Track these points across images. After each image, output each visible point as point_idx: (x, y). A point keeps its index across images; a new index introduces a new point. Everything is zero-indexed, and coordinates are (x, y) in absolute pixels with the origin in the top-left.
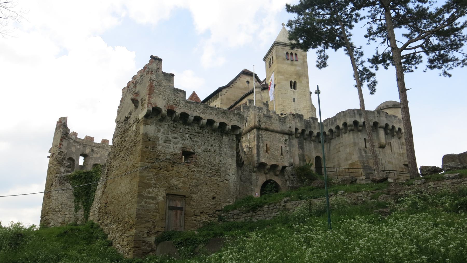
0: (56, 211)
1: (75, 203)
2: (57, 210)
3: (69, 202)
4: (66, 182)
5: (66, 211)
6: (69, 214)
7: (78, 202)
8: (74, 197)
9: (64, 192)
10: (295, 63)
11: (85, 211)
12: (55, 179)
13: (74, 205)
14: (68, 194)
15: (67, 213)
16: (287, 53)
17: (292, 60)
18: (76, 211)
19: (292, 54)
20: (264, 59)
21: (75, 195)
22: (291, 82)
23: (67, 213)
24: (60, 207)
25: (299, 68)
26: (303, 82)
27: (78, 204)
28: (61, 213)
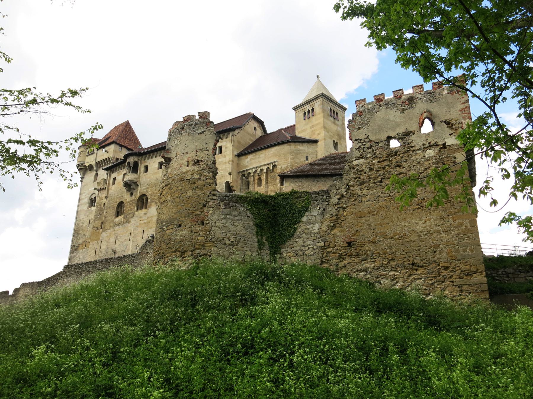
0: (225, 244)
1: (257, 237)
2: (227, 243)
3: (248, 234)
4: (237, 205)
5: (244, 246)
6: (250, 250)
7: (262, 236)
8: (255, 229)
9: (236, 218)
10: (337, 122)
11: (271, 250)
12: (210, 197)
13: (256, 240)
14: (245, 222)
15: (248, 249)
16: (331, 109)
17: (334, 119)
18: (260, 248)
19: (334, 112)
20: (295, 109)
21: (257, 225)
22: (334, 141)
23: (248, 249)
24: (232, 239)
25: (340, 129)
26: (343, 145)
27: (262, 239)
28: (236, 248)
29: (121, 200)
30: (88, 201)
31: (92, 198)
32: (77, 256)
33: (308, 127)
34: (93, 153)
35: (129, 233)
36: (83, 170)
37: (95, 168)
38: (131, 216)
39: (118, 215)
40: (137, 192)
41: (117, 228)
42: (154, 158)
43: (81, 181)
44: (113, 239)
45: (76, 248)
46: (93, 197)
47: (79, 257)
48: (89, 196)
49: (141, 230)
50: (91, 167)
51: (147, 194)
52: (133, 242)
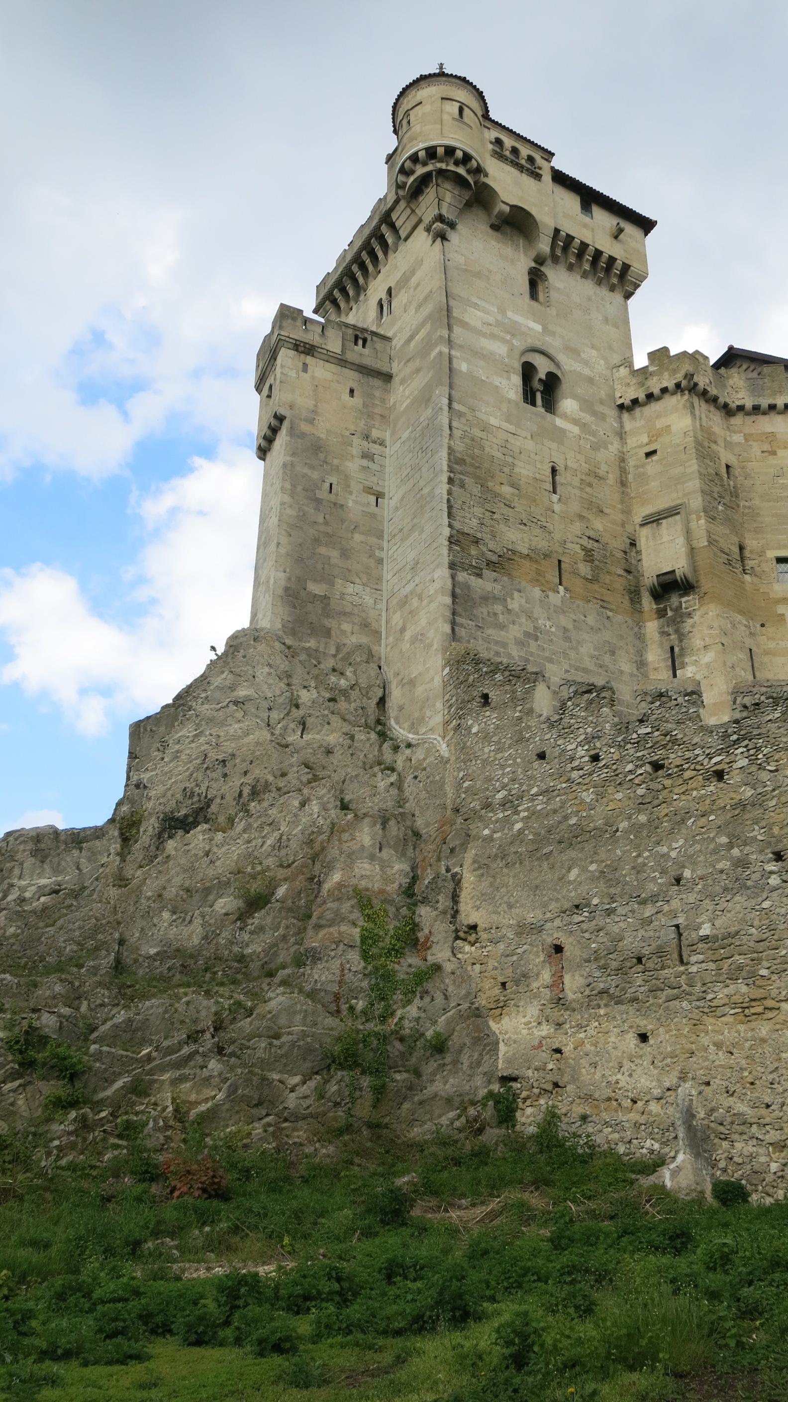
36: (467, 195)
37: (544, 246)
45: (494, 558)
48: (519, 344)
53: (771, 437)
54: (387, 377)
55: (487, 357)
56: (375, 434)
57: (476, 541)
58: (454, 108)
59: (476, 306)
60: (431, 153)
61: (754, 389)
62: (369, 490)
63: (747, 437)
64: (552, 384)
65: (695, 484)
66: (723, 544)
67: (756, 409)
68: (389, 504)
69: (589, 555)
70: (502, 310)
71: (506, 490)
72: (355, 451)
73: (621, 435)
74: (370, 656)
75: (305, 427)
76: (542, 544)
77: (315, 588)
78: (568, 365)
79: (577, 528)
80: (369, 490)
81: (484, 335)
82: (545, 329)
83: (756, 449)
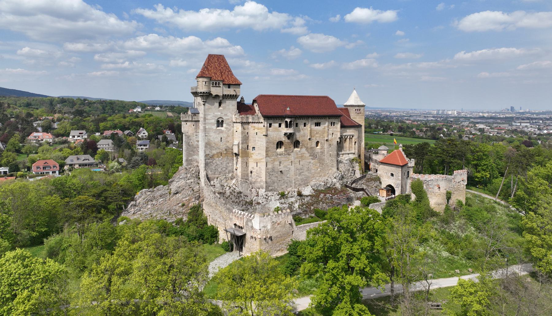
29: (280, 140)
30: (216, 122)
31: (219, 121)
32: (214, 162)
33: (358, 117)
34: (220, 87)
35: (290, 161)
37: (221, 99)
38: (290, 151)
39: (277, 148)
40: (293, 138)
41: (279, 156)
42: (301, 120)
43: (204, 104)
44: (277, 163)
46: (220, 120)
47: (216, 163)
48: (216, 118)
49: (298, 160)
50: (217, 96)
51: (300, 140)
52: (294, 166)
53: (254, 127)
54: (199, 121)
55: (211, 124)
56: (198, 131)
57: (209, 155)
58: (204, 83)
59: (210, 115)
60: (201, 92)
61: (253, 119)
62: (197, 141)
63: (251, 127)
64: (222, 121)
65: (241, 139)
66: (244, 147)
67: (253, 122)
68: (200, 143)
69: (226, 150)
70: (214, 113)
71: (214, 145)
72: (195, 135)
73: (233, 127)
74: (198, 166)
75: (187, 134)
76: (218, 151)
77: (190, 158)
78: (225, 118)
79: (225, 146)
80: (197, 141)
81: (210, 120)
82: (221, 113)
83: (252, 128)
